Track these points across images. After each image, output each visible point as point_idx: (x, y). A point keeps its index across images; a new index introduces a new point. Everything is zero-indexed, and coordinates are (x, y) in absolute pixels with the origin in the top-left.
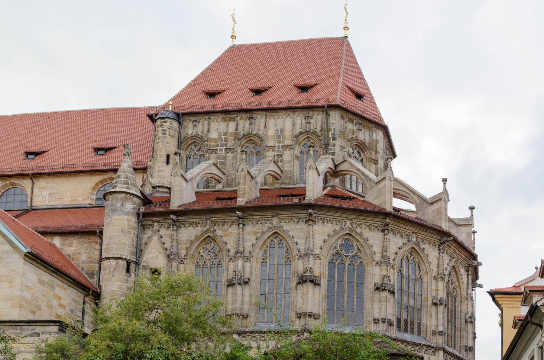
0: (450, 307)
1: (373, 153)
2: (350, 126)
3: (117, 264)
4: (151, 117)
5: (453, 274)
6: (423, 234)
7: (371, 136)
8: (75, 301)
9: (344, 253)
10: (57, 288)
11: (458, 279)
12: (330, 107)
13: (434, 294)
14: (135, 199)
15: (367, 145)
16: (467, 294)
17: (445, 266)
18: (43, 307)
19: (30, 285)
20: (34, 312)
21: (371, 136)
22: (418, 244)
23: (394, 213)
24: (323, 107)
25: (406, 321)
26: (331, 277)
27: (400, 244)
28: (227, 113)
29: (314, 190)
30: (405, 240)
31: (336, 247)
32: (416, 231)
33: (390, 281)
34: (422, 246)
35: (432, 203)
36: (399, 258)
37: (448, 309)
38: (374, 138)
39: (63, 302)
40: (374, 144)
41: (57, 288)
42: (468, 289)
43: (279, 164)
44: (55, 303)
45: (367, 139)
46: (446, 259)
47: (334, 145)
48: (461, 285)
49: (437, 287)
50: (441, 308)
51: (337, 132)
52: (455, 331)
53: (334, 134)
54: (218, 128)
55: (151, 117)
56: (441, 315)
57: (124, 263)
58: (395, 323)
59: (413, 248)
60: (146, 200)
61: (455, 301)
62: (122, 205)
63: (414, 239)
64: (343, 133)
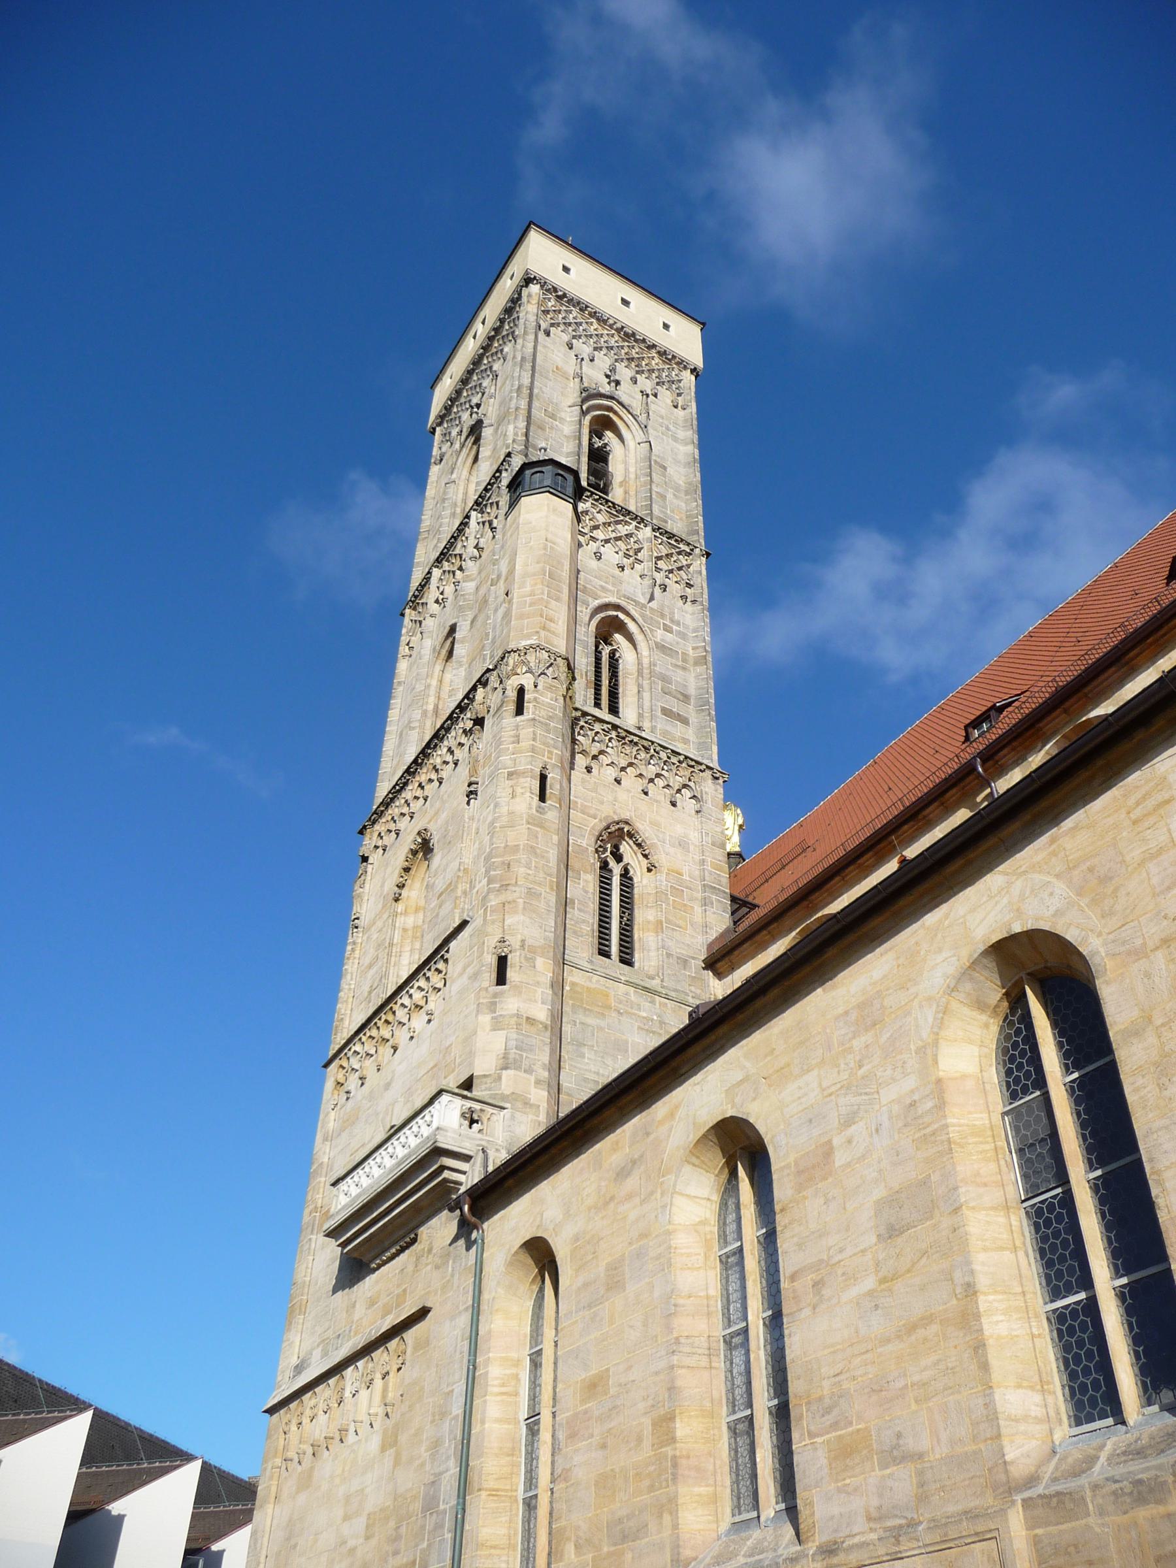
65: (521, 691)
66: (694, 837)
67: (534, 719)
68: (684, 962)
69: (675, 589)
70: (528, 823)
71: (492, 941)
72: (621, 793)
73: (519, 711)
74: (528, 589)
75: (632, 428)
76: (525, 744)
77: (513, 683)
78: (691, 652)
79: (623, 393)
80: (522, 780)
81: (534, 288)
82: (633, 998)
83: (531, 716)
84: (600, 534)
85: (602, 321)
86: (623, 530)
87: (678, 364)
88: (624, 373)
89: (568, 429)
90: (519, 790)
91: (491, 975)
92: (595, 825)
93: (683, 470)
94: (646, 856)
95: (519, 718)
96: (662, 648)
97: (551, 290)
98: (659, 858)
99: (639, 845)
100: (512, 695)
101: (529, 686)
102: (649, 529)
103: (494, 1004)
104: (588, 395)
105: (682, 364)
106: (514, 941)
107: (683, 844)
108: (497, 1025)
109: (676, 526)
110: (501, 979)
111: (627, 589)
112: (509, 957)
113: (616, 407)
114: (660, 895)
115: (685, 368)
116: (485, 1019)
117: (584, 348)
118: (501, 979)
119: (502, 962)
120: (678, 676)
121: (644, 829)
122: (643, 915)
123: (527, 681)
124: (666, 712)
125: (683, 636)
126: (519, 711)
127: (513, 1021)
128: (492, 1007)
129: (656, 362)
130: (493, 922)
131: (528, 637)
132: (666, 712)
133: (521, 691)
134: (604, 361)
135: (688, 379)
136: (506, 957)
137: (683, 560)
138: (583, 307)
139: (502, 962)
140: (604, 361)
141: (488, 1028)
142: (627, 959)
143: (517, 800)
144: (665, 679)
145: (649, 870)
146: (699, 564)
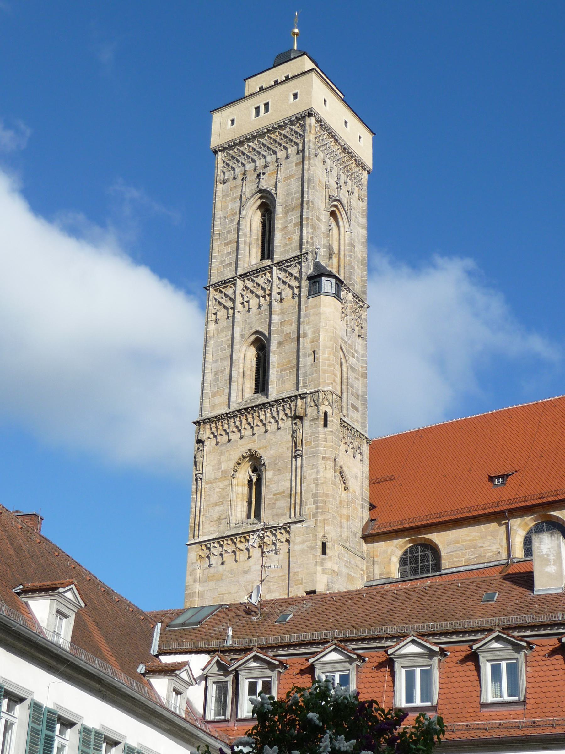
65: (326, 414)
67: (332, 432)
68: (355, 534)
70: (332, 484)
71: (320, 536)
73: (325, 425)
74: (327, 355)
75: (344, 219)
76: (329, 444)
77: (322, 409)
78: (360, 369)
80: (329, 462)
82: (343, 552)
83: (331, 430)
87: (362, 167)
90: (328, 467)
91: (320, 551)
93: (360, 247)
94: (345, 483)
95: (326, 429)
99: (343, 478)
100: (322, 415)
101: (329, 413)
102: (350, 294)
103: (322, 563)
105: (364, 167)
106: (329, 537)
108: (324, 572)
110: (324, 553)
112: (327, 543)
113: (340, 206)
115: (365, 169)
116: (319, 568)
118: (324, 553)
119: (324, 545)
123: (329, 410)
126: (325, 425)
127: (330, 571)
128: (322, 564)
130: (320, 527)
131: (328, 384)
133: (326, 414)
135: (365, 175)
136: (325, 543)
139: (324, 545)
141: (321, 572)
143: (327, 471)
145: (345, 490)
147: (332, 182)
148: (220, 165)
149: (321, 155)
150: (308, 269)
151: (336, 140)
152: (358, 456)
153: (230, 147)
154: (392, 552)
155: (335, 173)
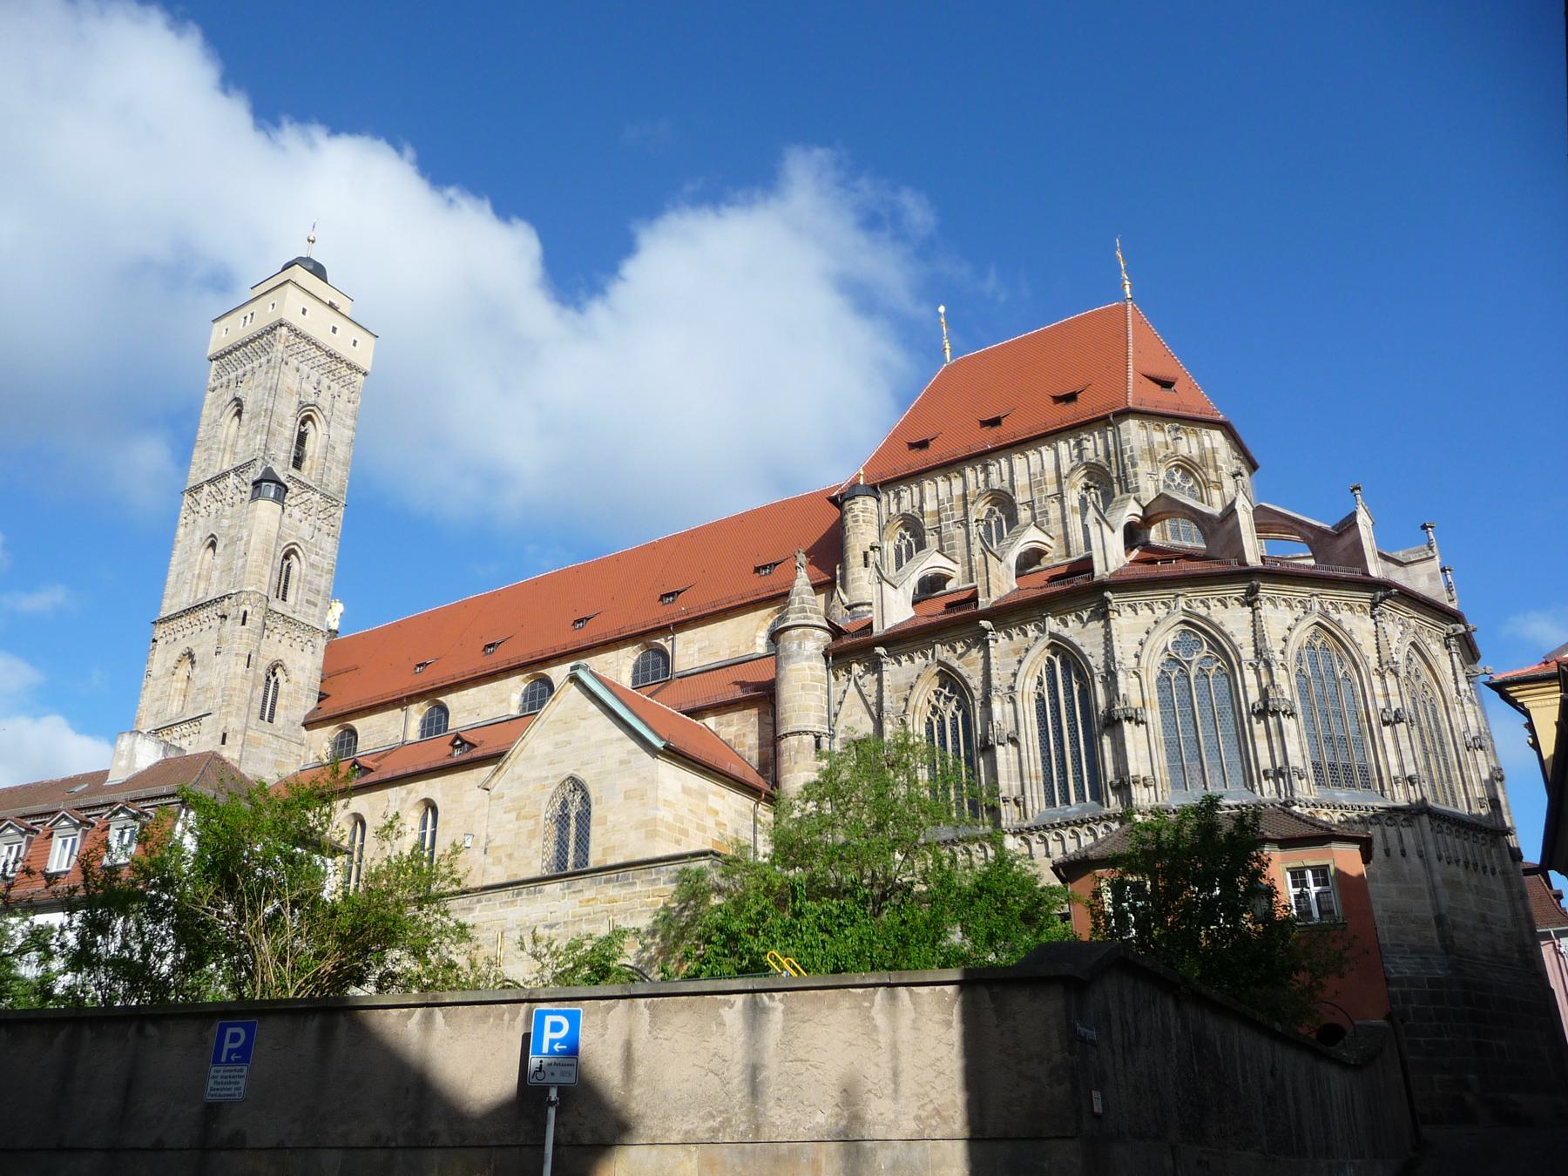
0: (1424, 724)
1: (1211, 471)
2: (1158, 437)
3: (800, 742)
4: (833, 500)
5: (1417, 658)
6: (1331, 595)
7: (1201, 444)
8: (741, 814)
9: (1183, 658)
10: (711, 797)
11: (1430, 667)
12: (1116, 415)
13: (1381, 704)
14: (819, 632)
15: (1197, 460)
16: (1458, 693)
17: (1393, 646)
18: (692, 831)
19: (670, 798)
20: (678, 842)
21: (1201, 444)
22: (1325, 614)
23: (1267, 567)
24: (1107, 417)
25: (1332, 766)
26: (1166, 703)
27: (1290, 621)
28: (949, 467)
29: (1112, 556)
30: (1299, 611)
31: (1166, 649)
32: (1316, 591)
33: (1282, 693)
34: (1335, 616)
35: (1340, 535)
36: (1293, 648)
37: (1421, 729)
38: (1207, 444)
39: (722, 818)
40: (1209, 455)
41: (711, 797)
42: (1456, 682)
43: (1045, 527)
44: (710, 822)
45: (1195, 452)
46: (1393, 629)
47: (1136, 475)
48: (1440, 678)
49: (1385, 688)
50: (1401, 727)
51: (1137, 453)
52: (1448, 771)
53: (1132, 457)
54: (936, 494)
55: (833, 500)
56: (1405, 744)
57: (811, 739)
58: (1310, 771)
59: (1318, 624)
60: (836, 632)
61: (1434, 712)
62: (800, 646)
63: (1317, 607)
64: (1151, 452)
66: (309, 665)
69: (325, 528)
72: (281, 648)
79: (320, 401)
81: (284, 329)
84: (293, 502)
85: (318, 347)
86: (305, 496)
88: (325, 381)
89: (287, 433)
92: (267, 663)
93: (344, 448)
96: (312, 565)
97: (292, 330)
98: (292, 677)
104: (302, 405)
107: (303, 669)
109: (333, 488)
111: (301, 533)
114: (289, 694)
117: (305, 368)
120: (317, 581)
121: (287, 663)
122: (279, 701)
124: (308, 602)
125: (324, 557)
129: (345, 371)
132: (308, 602)
134: (315, 376)
137: (333, 510)
138: (309, 340)
140: (315, 376)
142: (270, 721)
144: (311, 583)
146: (340, 513)
147: (308, 388)
148: (213, 372)
149: (294, 362)
150: (255, 473)
151: (318, 347)
152: (309, 649)
153: (222, 356)
154: (324, 738)
155: (314, 379)
